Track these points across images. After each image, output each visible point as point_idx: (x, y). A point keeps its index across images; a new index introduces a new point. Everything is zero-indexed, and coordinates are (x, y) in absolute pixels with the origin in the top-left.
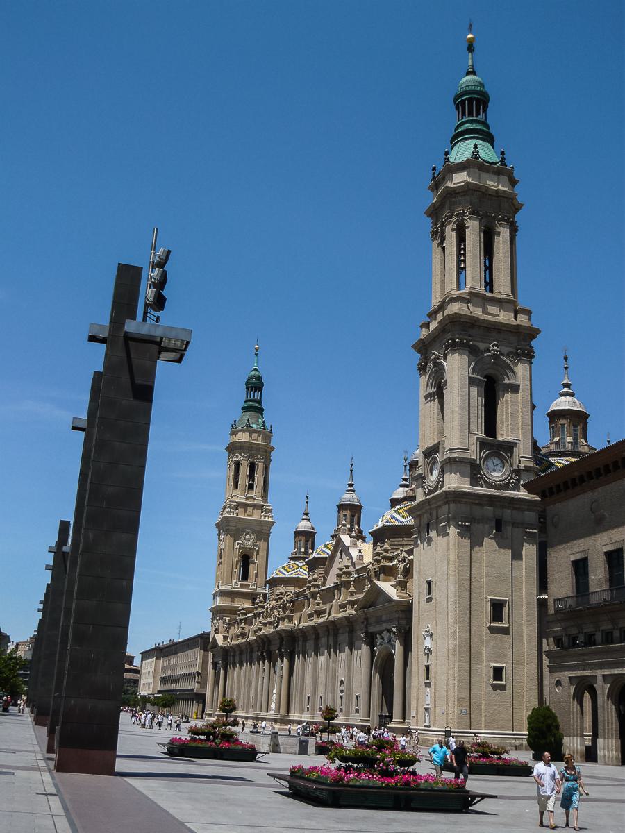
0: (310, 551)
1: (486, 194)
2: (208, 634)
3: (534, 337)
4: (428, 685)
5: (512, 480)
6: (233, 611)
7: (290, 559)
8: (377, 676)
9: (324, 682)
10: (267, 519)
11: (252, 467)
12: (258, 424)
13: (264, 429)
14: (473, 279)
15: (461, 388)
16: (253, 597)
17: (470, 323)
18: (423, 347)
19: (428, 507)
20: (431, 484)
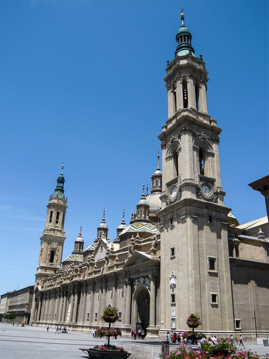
0: (81, 250)
1: (195, 70)
2: (33, 287)
3: (219, 133)
4: (173, 305)
5: (214, 198)
6: (47, 276)
7: (73, 253)
8: (135, 302)
9: (98, 306)
10: (63, 236)
11: (58, 214)
12: (61, 196)
13: (64, 198)
14: (192, 104)
15: (190, 150)
16: (55, 270)
17: (192, 121)
18: (164, 137)
19: (172, 210)
20: (171, 199)
